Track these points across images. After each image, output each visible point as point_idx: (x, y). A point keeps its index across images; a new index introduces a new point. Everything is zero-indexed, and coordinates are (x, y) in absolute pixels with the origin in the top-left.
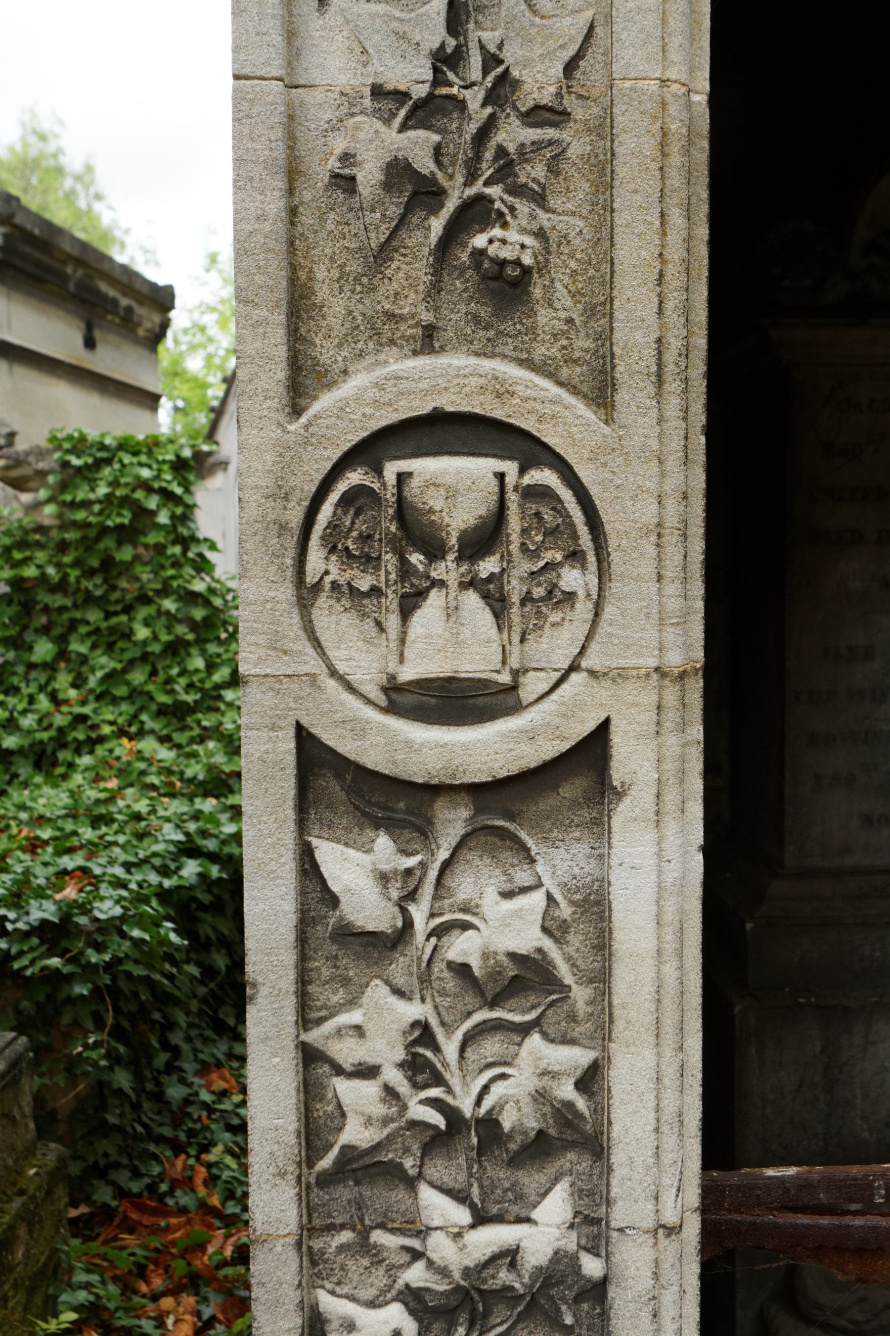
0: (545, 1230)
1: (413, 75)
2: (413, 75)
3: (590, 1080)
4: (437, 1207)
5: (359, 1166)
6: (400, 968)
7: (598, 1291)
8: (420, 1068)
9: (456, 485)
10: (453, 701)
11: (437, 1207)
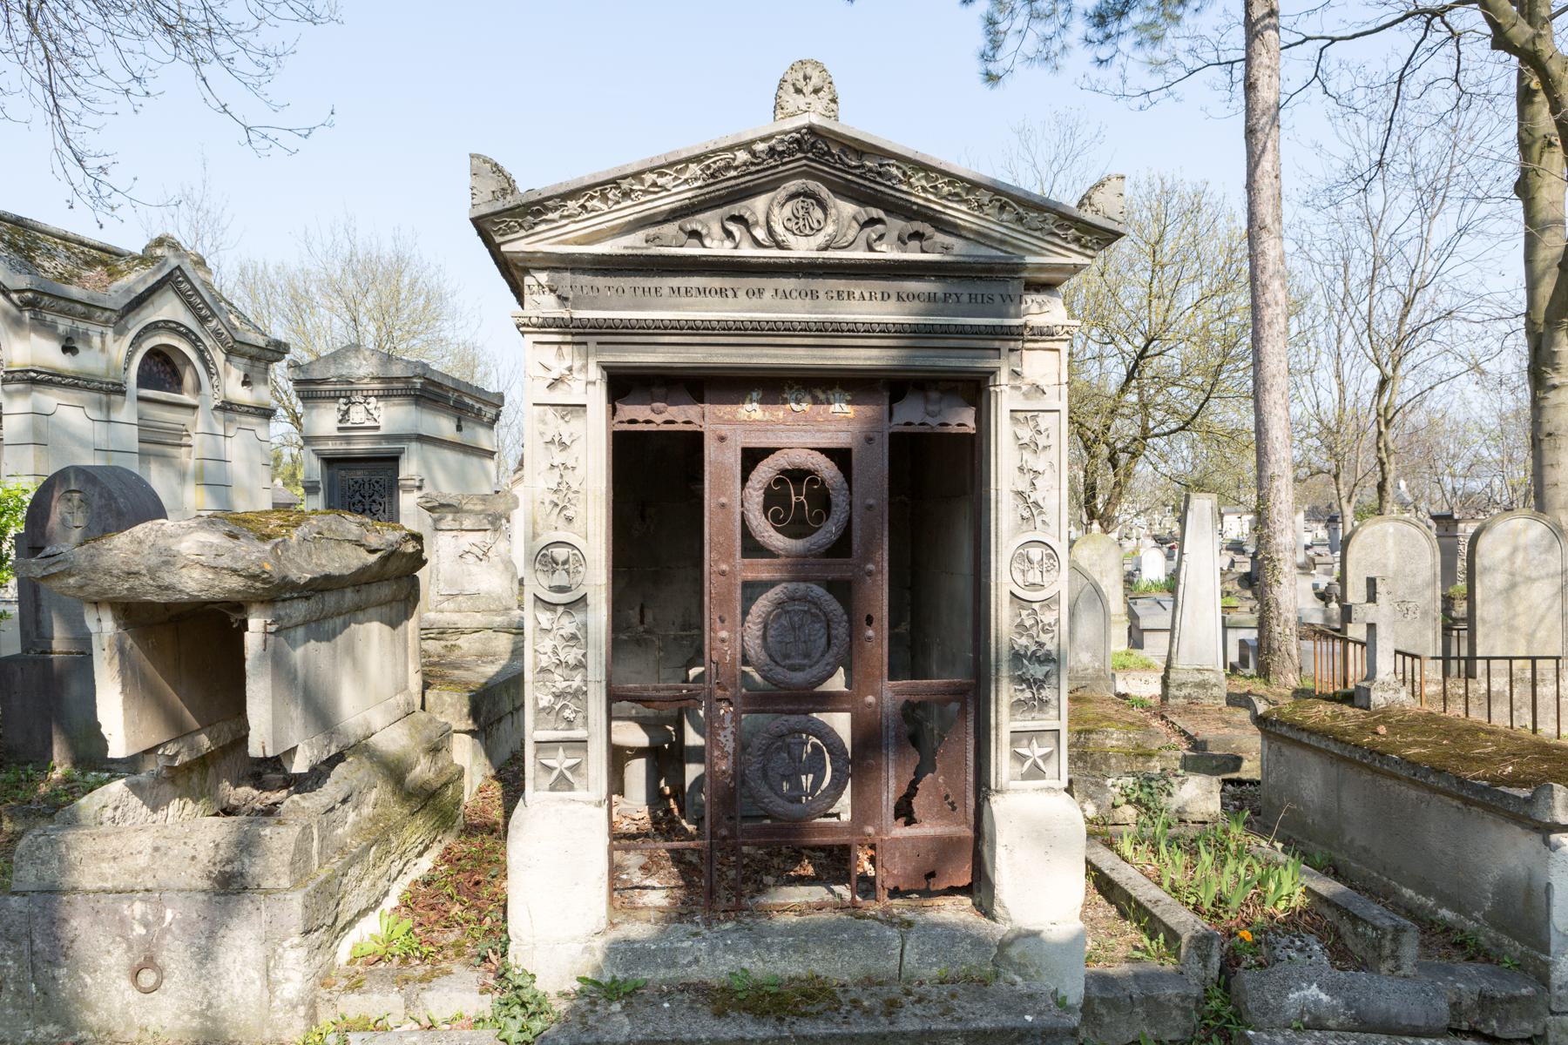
0: (577, 682)
1: (555, 486)
2: (555, 486)
3: (584, 655)
4: (557, 677)
5: (543, 670)
6: (551, 635)
7: (585, 693)
8: (555, 653)
9: (560, 553)
10: (561, 589)
11: (557, 677)
